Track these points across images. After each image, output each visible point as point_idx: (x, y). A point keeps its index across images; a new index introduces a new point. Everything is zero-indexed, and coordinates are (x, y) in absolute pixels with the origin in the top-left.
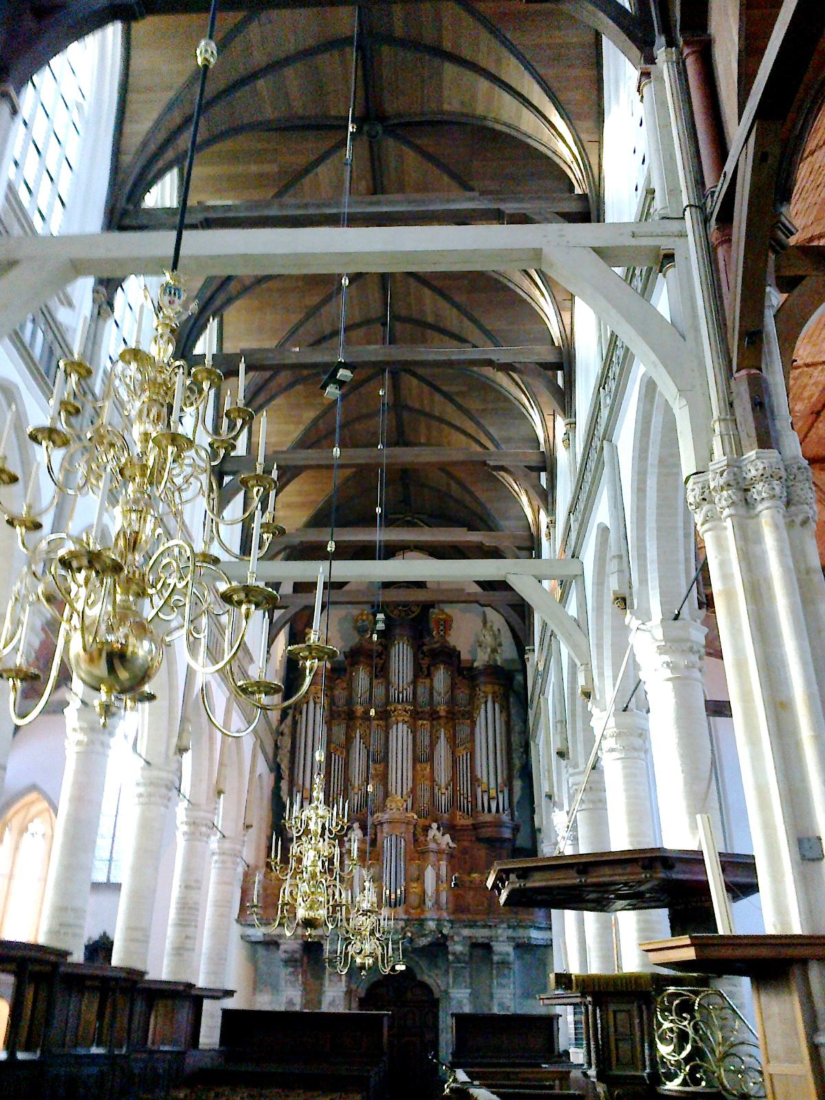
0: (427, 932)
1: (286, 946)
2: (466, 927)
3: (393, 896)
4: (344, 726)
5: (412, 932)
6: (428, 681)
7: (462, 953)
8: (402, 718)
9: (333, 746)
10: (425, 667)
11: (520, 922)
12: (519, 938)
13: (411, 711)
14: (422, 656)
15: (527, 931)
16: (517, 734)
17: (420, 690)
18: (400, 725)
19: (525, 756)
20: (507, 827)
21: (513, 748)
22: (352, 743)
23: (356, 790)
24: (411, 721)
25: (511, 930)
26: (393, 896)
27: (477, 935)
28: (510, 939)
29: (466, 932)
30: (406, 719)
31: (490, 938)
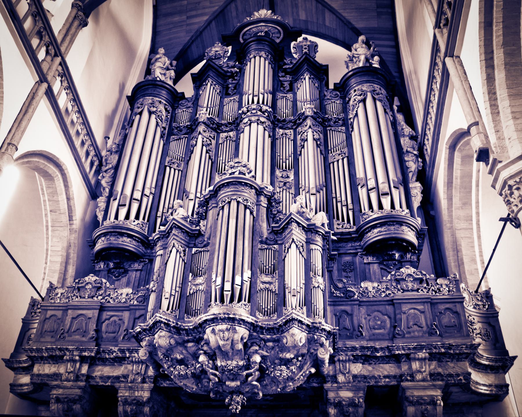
0: (290, 356)
1: (61, 391)
2: (356, 359)
3: (228, 286)
4: (184, 142)
5: (263, 357)
6: (290, 96)
7: (352, 403)
8: (257, 118)
9: (168, 159)
10: (286, 84)
11: (450, 349)
12: (450, 375)
13: (269, 112)
14: (283, 74)
15: (460, 364)
16: (407, 139)
17: (280, 103)
18: (254, 125)
19: (420, 160)
20: (409, 225)
21: (405, 150)
22: (192, 152)
23: (192, 196)
24: (268, 123)
25: (434, 363)
26: (228, 286)
27: (376, 374)
28: (434, 376)
29: (357, 368)
30: (262, 119)
31: (400, 378)
